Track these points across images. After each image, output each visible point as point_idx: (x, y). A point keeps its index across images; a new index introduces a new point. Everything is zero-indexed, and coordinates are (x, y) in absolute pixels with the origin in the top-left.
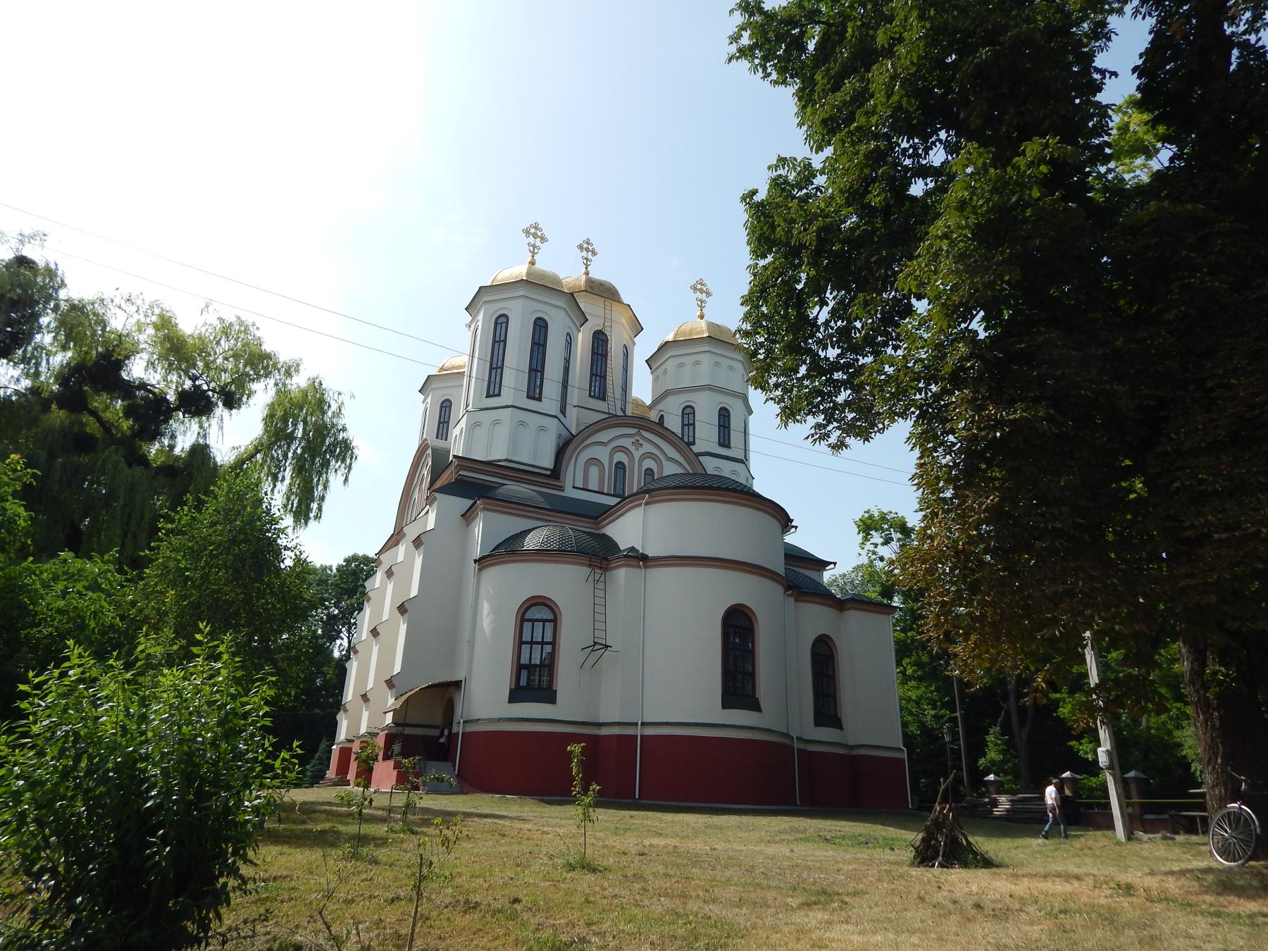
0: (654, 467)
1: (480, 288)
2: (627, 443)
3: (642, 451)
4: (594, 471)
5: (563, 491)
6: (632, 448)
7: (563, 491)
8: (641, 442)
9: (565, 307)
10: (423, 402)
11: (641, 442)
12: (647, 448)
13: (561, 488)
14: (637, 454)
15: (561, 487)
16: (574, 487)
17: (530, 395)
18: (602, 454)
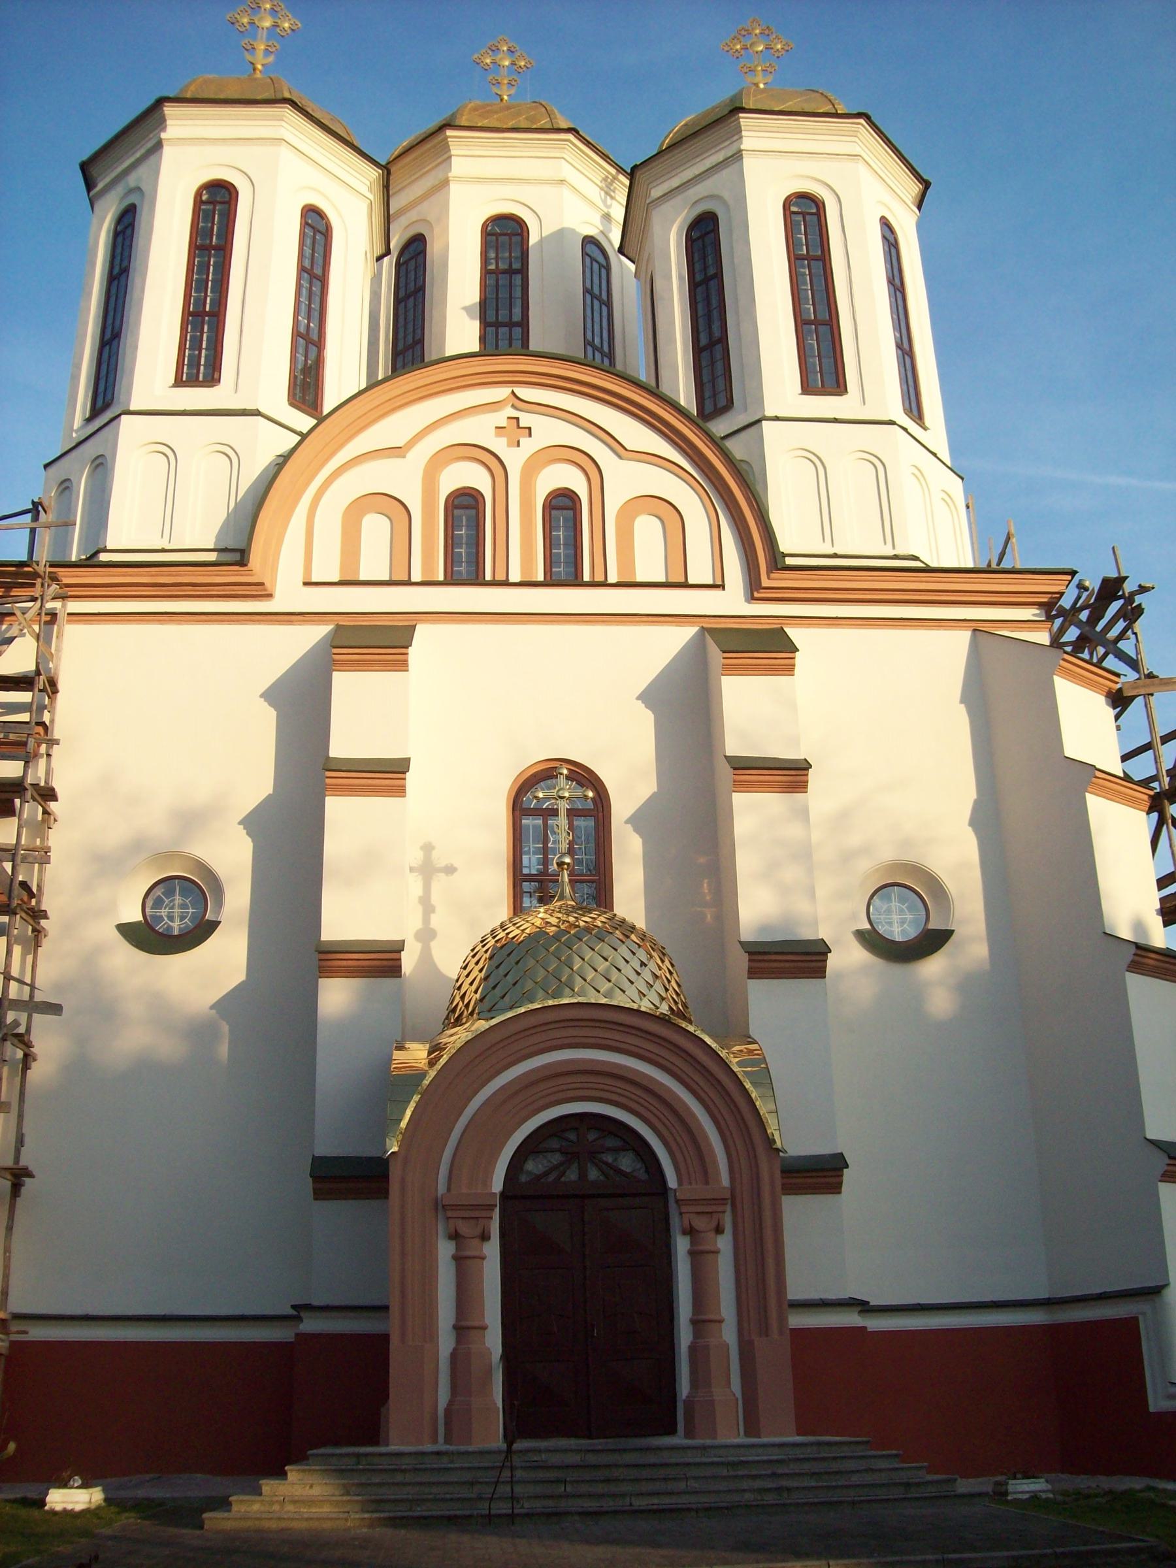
0: (577, 483)
1: (84, 167)
3: (530, 446)
5: (270, 596)
6: (499, 445)
7: (270, 596)
8: (526, 419)
11: (526, 419)
13: (260, 591)
14: (515, 460)
16: (306, 584)
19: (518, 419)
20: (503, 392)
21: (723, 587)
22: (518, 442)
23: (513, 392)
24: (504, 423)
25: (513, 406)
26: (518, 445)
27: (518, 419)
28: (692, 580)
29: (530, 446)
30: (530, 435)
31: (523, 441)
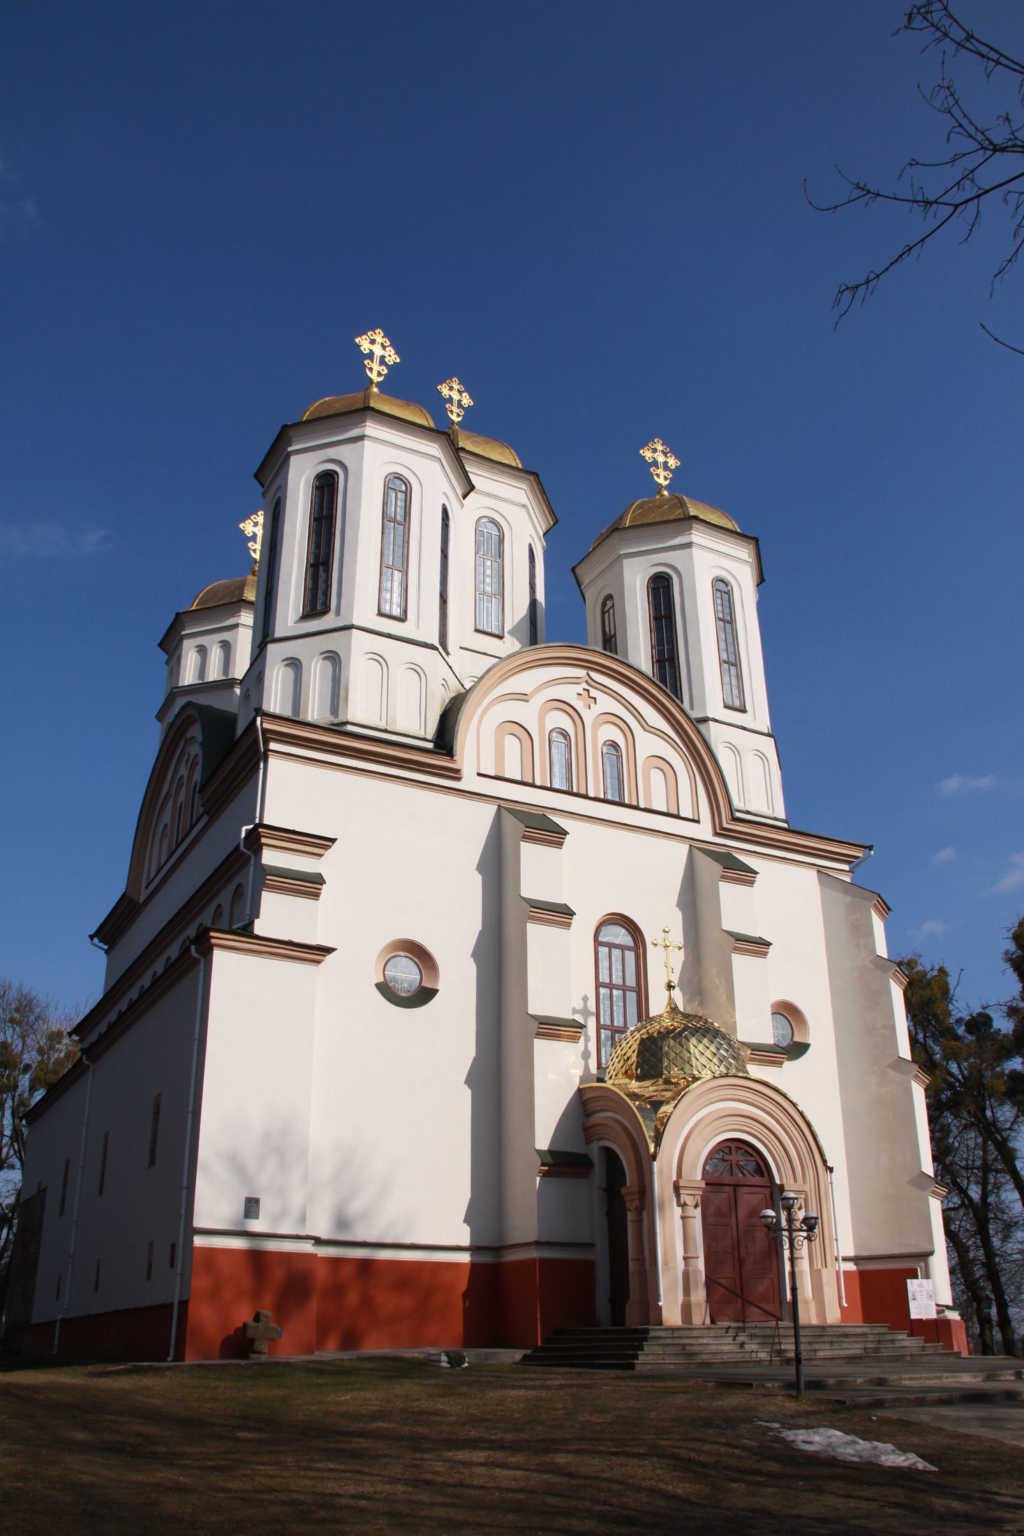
0: (620, 741)
2: (569, 693)
3: (597, 709)
4: (512, 745)
7: (459, 779)
8: (593, 693)
9: (439, 456)
10: (167, 662)
11: (593, 693)
12: (606, 704)
13: (455, 774)
14: (589, 716)
15: (457, 771)
16: (479, 774)
17: (386, 609)
18: (527, 714)
19: (588, 691)
20: (582, 673)
21: (698, 822)
22: (589, 706)
23: (588, 673)
24: (581, 692)
25: (586, 682)
26: (590, 708)
27: (588, 691)
28: (682, 815)
29: (597, 709)
30: (595, 703)
31: (592, 706)
